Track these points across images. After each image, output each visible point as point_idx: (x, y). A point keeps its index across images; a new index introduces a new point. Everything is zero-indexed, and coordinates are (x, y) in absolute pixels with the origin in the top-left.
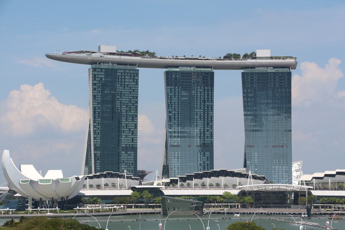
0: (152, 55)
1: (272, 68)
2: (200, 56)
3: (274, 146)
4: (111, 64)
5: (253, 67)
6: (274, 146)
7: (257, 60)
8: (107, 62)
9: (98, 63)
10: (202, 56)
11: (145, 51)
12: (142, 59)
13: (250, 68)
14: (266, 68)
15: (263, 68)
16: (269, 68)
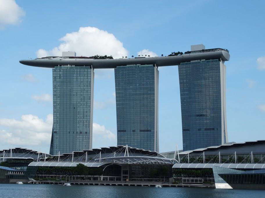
0: (111, 58)
1: (205, 60)
2: (146, 55)
3: (206, 129)
4: (70, 66)
5: (188, 60)
6: (206, 129)
7: (190, 54)
8: (66, 64)
9: (59, 65)
10: (147, 55)
11: (104, 55)
12: (94, 60)
13: (187, 62)
14: (199, 60)
15: (197, 61)
16: (202, 60)
